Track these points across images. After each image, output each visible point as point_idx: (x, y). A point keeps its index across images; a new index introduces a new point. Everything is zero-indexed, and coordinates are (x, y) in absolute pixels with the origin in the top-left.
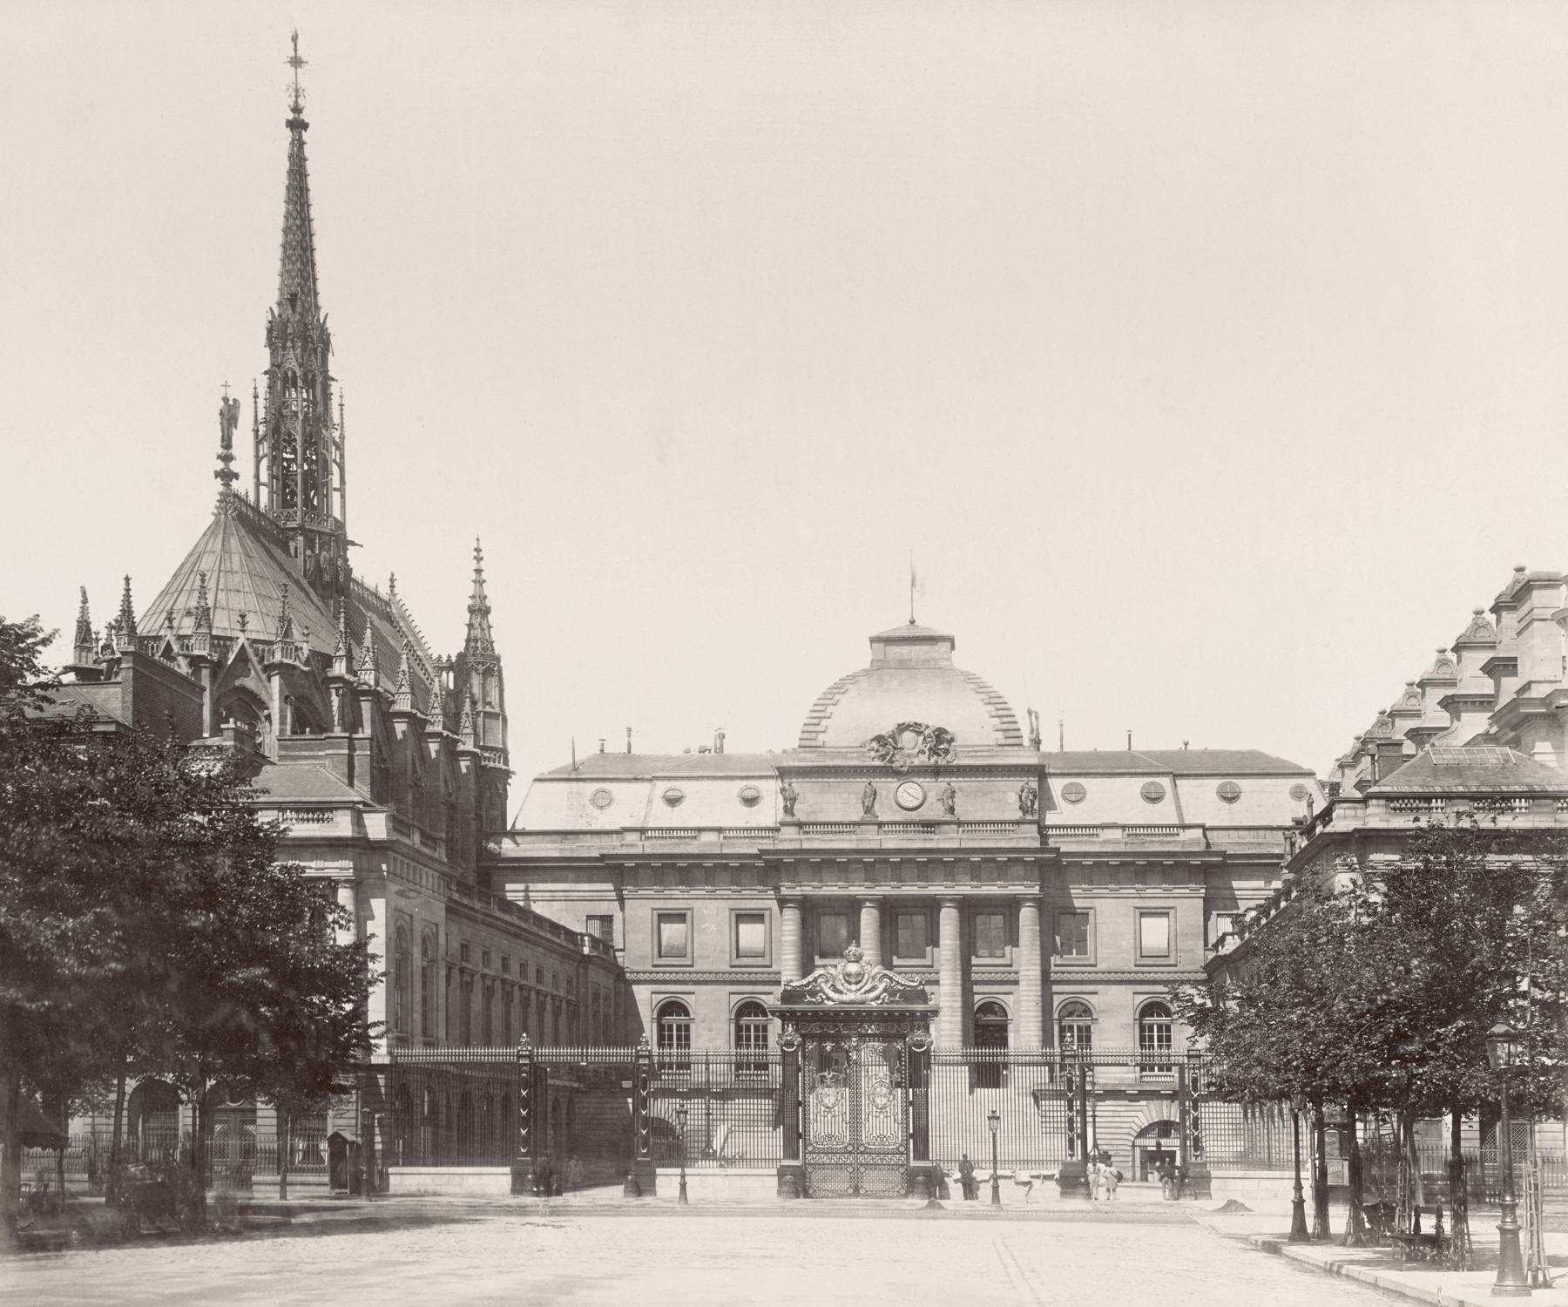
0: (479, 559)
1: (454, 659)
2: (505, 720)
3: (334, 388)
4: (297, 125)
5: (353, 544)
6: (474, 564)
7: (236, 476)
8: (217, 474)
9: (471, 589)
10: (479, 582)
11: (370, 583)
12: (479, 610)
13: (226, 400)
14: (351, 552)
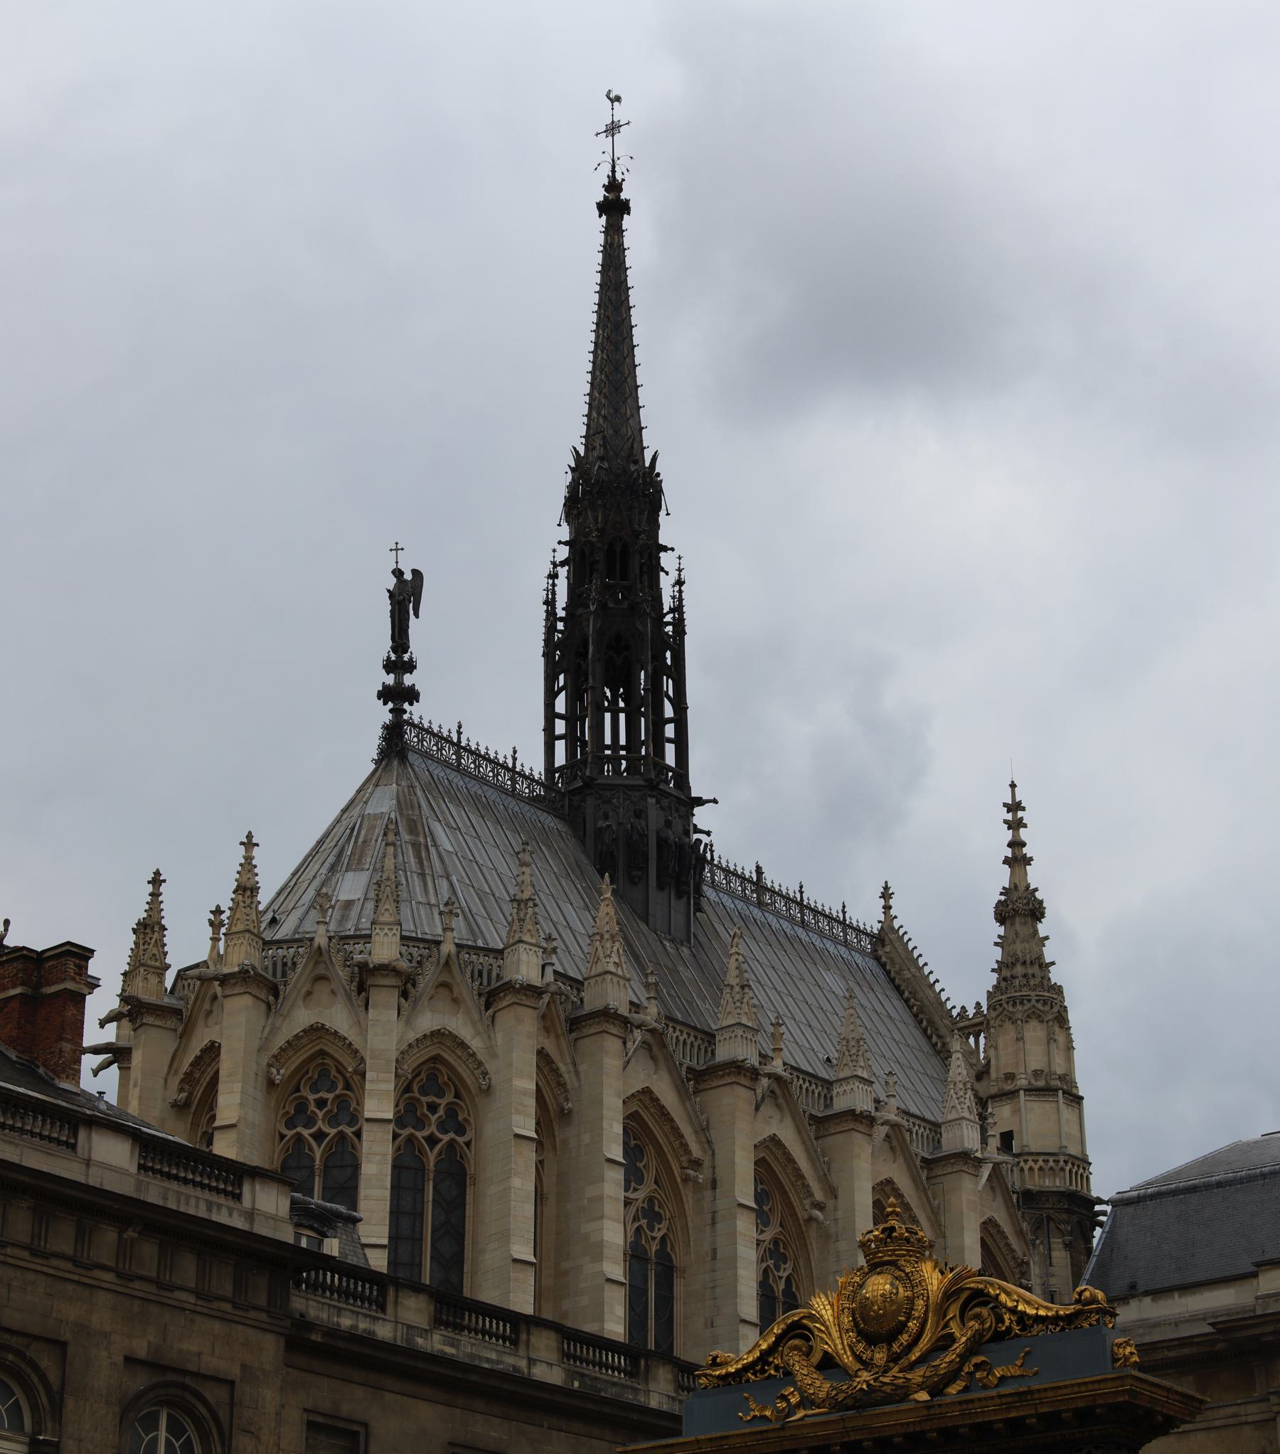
0: (1016, 825)
1: (985, 1009)
2: (1076, 1100)
3: (666, 560)
4: (614, 207)
5: (700, 802)
6: (1008, 835)
7: (412, 695)
8: (386, 694)
9: (1003, 876)
10: (1018, 859)
11: (822, 896)
12: (1020, 910)
13: (398, 573)
14: (701, 817)
